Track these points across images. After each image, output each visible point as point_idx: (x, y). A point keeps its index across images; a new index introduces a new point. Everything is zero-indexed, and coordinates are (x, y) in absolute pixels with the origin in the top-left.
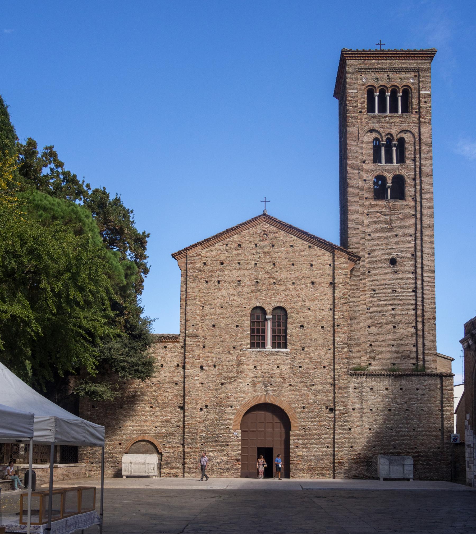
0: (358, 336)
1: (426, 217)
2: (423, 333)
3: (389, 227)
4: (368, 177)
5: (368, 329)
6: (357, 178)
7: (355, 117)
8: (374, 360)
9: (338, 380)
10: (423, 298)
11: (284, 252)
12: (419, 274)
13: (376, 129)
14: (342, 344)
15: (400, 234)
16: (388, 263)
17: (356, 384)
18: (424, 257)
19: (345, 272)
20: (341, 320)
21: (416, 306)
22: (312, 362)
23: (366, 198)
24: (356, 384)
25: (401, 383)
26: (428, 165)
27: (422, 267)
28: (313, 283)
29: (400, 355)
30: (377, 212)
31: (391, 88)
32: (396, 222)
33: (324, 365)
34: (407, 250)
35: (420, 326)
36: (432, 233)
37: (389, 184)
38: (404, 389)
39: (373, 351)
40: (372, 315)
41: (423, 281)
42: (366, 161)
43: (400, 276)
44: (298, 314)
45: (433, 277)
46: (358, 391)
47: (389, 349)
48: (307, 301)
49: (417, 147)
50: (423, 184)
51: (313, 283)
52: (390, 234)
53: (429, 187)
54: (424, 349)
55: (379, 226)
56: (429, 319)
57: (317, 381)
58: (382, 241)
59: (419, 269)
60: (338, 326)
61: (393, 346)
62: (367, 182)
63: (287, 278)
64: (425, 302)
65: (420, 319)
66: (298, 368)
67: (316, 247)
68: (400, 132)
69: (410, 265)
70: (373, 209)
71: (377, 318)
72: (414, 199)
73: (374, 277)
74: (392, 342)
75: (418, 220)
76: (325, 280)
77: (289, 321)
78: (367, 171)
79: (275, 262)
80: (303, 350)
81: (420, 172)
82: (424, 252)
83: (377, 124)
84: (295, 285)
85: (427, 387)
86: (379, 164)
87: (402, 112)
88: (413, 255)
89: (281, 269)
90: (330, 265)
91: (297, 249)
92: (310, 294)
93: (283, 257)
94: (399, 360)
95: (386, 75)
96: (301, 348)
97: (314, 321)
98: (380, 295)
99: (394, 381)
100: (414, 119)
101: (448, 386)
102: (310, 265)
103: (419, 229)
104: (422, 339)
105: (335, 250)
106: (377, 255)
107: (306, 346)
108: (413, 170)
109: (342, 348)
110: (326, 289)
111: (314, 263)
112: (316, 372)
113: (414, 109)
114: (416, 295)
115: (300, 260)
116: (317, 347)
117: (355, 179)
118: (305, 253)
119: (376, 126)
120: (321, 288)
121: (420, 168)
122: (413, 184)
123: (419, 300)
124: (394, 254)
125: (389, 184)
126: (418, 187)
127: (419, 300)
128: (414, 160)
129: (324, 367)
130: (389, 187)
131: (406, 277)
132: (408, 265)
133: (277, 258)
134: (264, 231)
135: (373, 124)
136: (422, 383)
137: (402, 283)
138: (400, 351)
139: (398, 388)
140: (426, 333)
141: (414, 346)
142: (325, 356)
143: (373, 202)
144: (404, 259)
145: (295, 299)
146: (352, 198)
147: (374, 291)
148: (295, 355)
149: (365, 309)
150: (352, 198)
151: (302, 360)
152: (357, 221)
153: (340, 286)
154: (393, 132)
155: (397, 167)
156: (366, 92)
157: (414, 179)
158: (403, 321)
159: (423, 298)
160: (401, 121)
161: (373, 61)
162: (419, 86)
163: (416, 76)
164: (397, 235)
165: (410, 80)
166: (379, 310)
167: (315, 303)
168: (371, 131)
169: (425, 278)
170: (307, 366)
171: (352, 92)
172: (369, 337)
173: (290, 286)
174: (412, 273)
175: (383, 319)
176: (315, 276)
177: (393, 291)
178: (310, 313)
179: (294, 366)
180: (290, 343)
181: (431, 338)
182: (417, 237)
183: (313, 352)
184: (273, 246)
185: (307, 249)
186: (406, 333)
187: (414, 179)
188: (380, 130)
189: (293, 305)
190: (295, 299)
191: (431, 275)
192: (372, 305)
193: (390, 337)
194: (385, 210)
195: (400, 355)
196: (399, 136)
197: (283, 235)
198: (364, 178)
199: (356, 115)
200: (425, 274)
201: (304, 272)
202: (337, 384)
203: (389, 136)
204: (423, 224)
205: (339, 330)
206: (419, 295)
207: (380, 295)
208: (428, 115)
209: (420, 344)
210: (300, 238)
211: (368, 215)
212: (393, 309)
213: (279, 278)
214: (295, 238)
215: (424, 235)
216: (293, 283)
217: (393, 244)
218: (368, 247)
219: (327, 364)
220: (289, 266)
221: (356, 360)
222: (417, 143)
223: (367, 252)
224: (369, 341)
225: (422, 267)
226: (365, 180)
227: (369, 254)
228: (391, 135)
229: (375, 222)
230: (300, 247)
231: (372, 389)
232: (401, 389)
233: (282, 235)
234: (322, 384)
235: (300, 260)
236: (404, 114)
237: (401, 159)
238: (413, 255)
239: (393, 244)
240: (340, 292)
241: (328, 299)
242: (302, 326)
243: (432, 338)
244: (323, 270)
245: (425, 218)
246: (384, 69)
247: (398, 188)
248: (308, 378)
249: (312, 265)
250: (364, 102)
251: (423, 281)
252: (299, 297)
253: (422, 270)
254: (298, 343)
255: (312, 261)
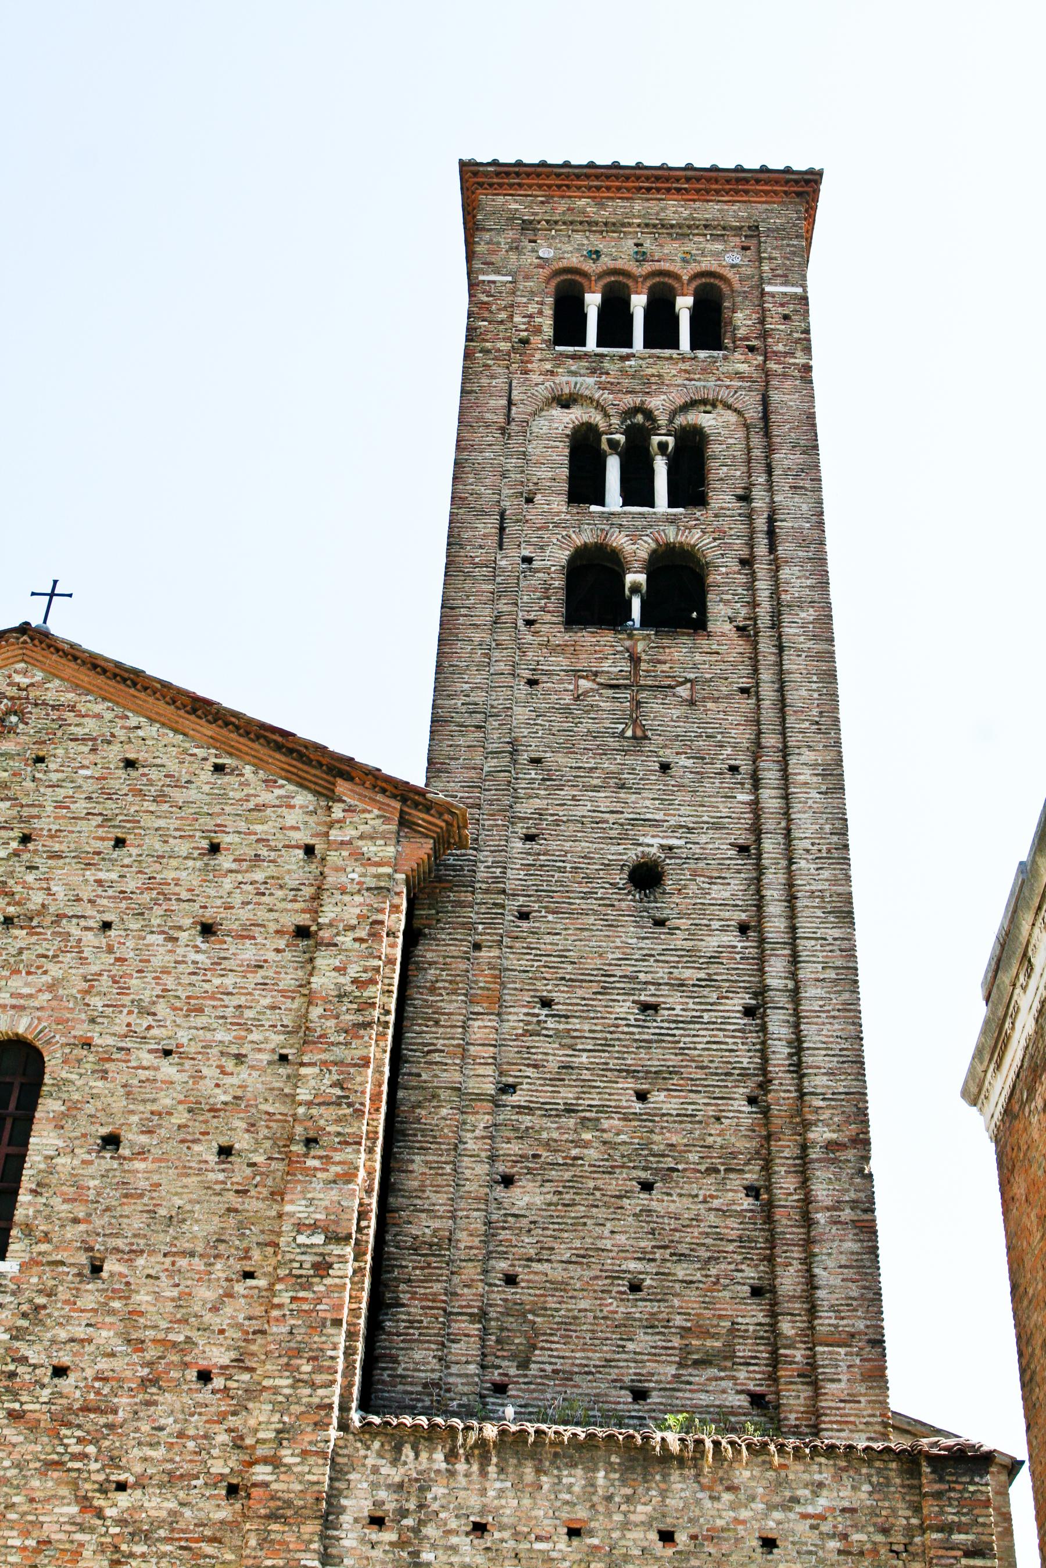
0: (437, 1224)
1: (804, 693)
2: (807, 1221)
3: (629, 733)
4: (542, 548)
5: (499, 1191)
6: (492, 542)
7: (499, 350)
8: (524, 1365)
9: (274, 1462)
10: (797, 1045)
11: (89, 786)
12: (776, 926)
13: (587, 393)
14: (319, 1239)
15: (683, 761)
16: (621, 878)
17: (382, 1494)
18: (799, 853)
19: (378, 876)
20: (330, 1113)
21: (764, 1085)
22: (139, 1345)
23: (529, 623)
24: (382, 1494)
25: (664, 1494)
26: (805, 507)
27: (791, 899)
28: (207, 930)
29: (676, 1342)
30: (577, 674)
31: (649, 283)
32: (664, 714)
33: (203, 1363)
34: (717, 827)
35: (786, 1184)
36: (829, 756)
37: (636, 578)
38: (681, 1538)
39: (516, 1311)
40: (527, 1120)
41: (794, 959)
42: (538, 497)
43: (678, 941)
44: (104, 1075)
45: (845, 945)
46: (393, 1537)
47: (612, 1304)
48: (162, 1009)
49: (757, 453)
50: (785, 573)
51: (207, 930)
52: (630, 760)
53: (809, 582)
54: (812, 1311)
55: (582, 729)
56: (831, 1146)
57: (145, 1459)
58: (596, 789)
59: (775, 909)
60: (310, 1142)
61: (635, 1287)
62: (536, 564)
63: (78, 900)
64: (808, 1059)
65: (786, 1150)
66: (45, 1374)
67: (248, 770)
68: (685, 408)
69: (732, 888)
70: (560, 662)
71: (555, 1135)
72: (746, 631)
73: (549, 939)
74: (632, 1265)
75: (769, 713)
76: (275, 915)
77: (48, 1107)
78: (539, 529)
79: (37, 824)
80: (96, 1270)
81: (771, 533)
82: (795, 834)
83: (591, 380)
84: (112, 933)
85: (826, 1527)
86: (594, 508)
87: (693, 347)
88: (743, 849)
89: (56, 856)
90: (309, 850)
91: (154, 774)
92: (186, 980)
93: (80, 807)
94: (672, 1370)
95: (630, 243)
96: (83, 1259)
97: (181, 1117)
98: (575, 1024)
99: (624, 1482)
100: (743, 367)
101: (961, 1528)
102: (205, 844)
103: (771, 740)
104: (797, 1253)
105: (339, 781)
106: (568, 846)
107: (117, 1250)
108: (741, 528)
109: (315, 1266)
110: (271, 956)
111: (225, 839)
112: (148, 1403)
113: (741, 339)
114: (763, 1028)
115: (161, 823)
116: (183, 1253)
117: (481, 547)
118: (192, 794)
119: (588, 384)
120: (248, 953)
121: (771, 520)
122: (742, 579)
123: (780, 1052)
124: (652, 844)
125: (636, 578)
126: (763, 586)
127: (780, 1052)
128: (745, 498)
129: (205, 1376)
130: (635, 589)
131: (711, 943)
132: (719, 893)
133: (49, 809)
134: (12, 699)
135: (573, 379)
136: (795, 1500)
137: (687, 973)
138: (678, 1321)
139: (648, 1525)
140: (821, 1217)
141: (756, 1292)
142: (215, 1309)
143: (561, 637)
144: (702, 864)
145: (97, 1002)
146: (463, 611)
147: (546, 1003)
148: (41, 1300)
149: (490, 1088)
150: (463, 611)
151: (80, 1332)
152: (479, 697)
153: (346, 940)
154: (657, 403)
155: (672, 520)
156: (551, 288)
157: (747, 563)
158: (693, 1157)
159: (797, 1045)
160: (686, 371)
161: (582, 202)
162: (761, 272)
163: (745, 248)
164: (665, 767)
165: (727, 258)
166: (567, 1094)
167: (201, 1021)
168: (566, 402)
169: (805, 946)
170: (103, 1364)
171: (494, 282)
172: (504, 1235)
173: (89, 937)
174: (743, 929)
175: (586, 1145)
176: (225, 894)
177: (645, 1007)
178: (168, 1069)
179: (23, 1360)
180: (28, 1230)
181: (850, 1245)
182: (763, 774)
183: (151, 1285)
184: (40, 760)
185: (206, 775)
186: (712, 1218)
187: (747, 563)
188: (607, 397)
189: (81, 1030)
190: (97, 1002)
191: (837, 933)
192: (530, 1072)
193: (621, 1239)
194: (614, 667)
195: (676, 1342)
196: (681, 420)
197: (98, 716)
198: (526, 553)
199: (504, 346)
200: (805, 926)
201: (170, 875)
202: (266, 1485)
203: (640, 418)
204: (790, 720)
205: (311, 1163)
206: (778, 1024)
207: (575, 1024)
208: (799, 354)
209: (789, 1281)
210: (176, 731)
211: (532, 683)
212: (642, 1096)
213: (38, 898)
214: (151, 731)
215: (793, 760)
216: (107, 926)
217: (648, 803)
218: (525, 808)
219: (218, 1356)
220: (98, 845)
221: (418, 1355)
222: (757, 440)
223: (521, 829)
224: (503, 1256)
225: (791, 899)
226: (527, 560)
227: (529, 838)
228: (649, 414)
229: (566, 711)
230: (173, 766)
231: (480, 1529)
232: (667, 1537)
233: (96, 714)
234: (172, 1479)
235: (161, 823)
236: (702, 354)
237: (690, 490)
238: (743, 849)
239: (648, 803)
240: (341, 970)
241: (273, 1008)
242: (112, 1141)
243: (855, 1247)
244: (272, 870)
245: (798, 695)
246: (623, 225)
247: (679, 593)
248: (95, 1442)
249: (215, 849)
250: (540, 313)
251: (794, 959)
252: (124, 990)
253: (792, 914)
254: (72, 1232)
255: (221, 828)
